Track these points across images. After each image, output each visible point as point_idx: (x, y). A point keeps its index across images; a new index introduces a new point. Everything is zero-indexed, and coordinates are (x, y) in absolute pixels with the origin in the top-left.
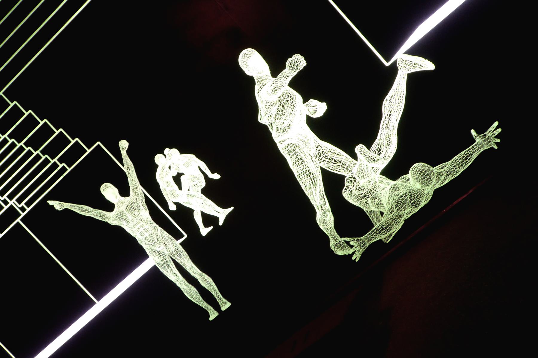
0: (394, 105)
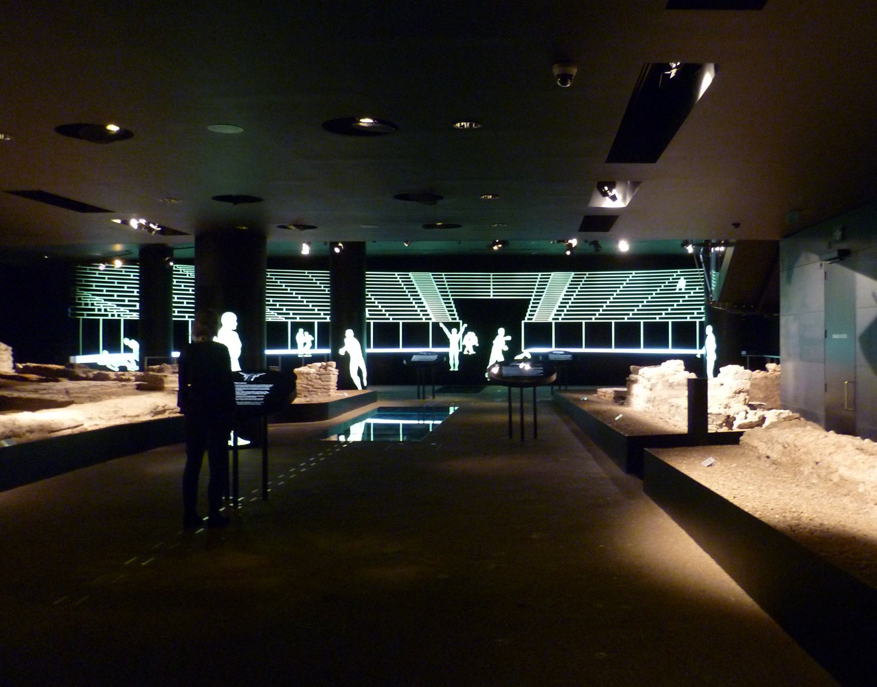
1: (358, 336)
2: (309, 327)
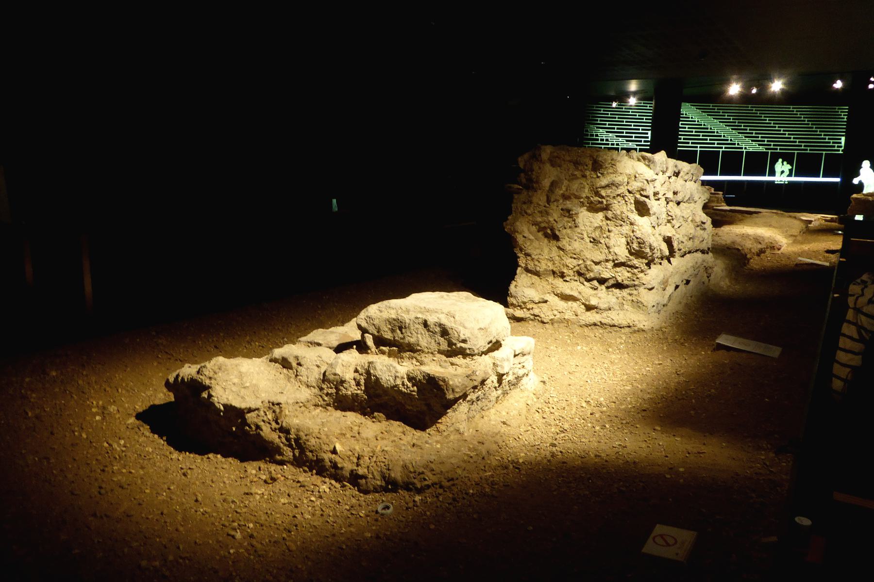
2: (788, 158)
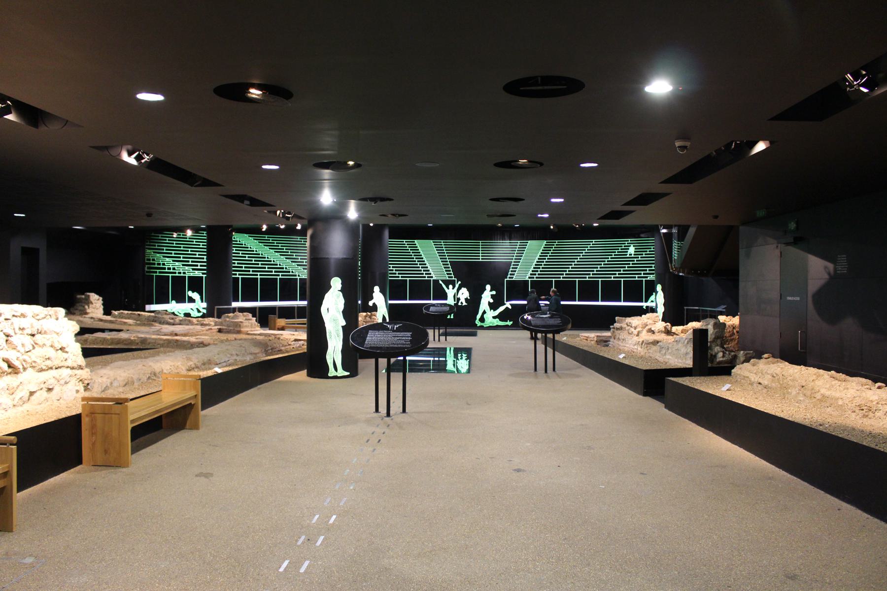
0: (502, 309)
1: (383, 291)
